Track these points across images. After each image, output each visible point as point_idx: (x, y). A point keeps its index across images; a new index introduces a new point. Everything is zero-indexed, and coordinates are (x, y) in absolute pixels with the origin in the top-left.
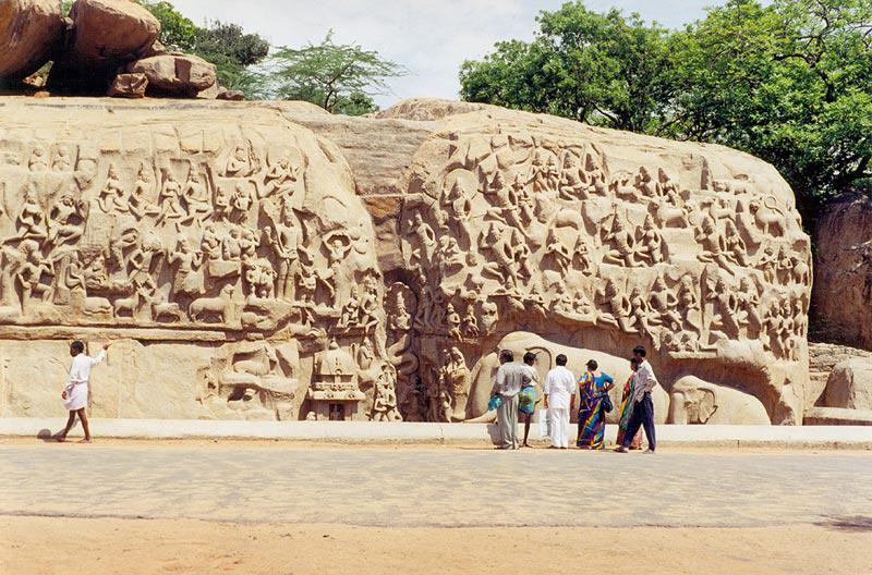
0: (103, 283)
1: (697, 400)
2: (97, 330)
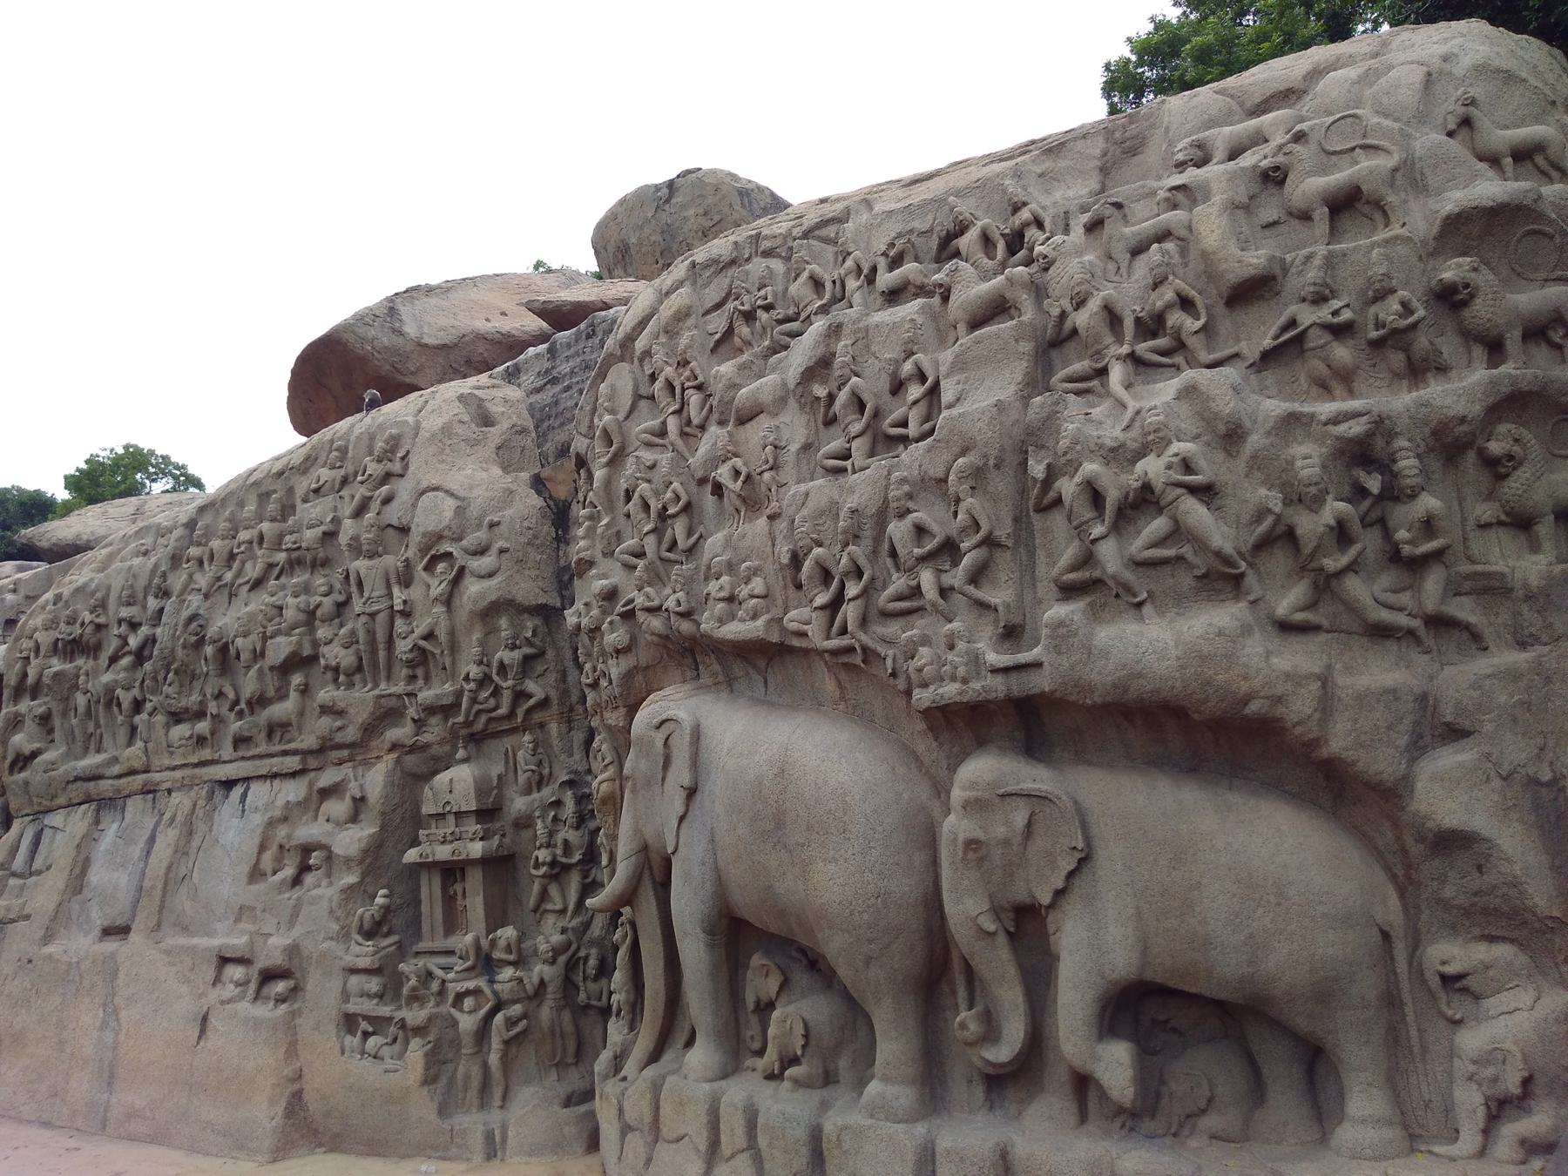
0: (183, 703)
1: (1000, 831)
2: (178, 774)
